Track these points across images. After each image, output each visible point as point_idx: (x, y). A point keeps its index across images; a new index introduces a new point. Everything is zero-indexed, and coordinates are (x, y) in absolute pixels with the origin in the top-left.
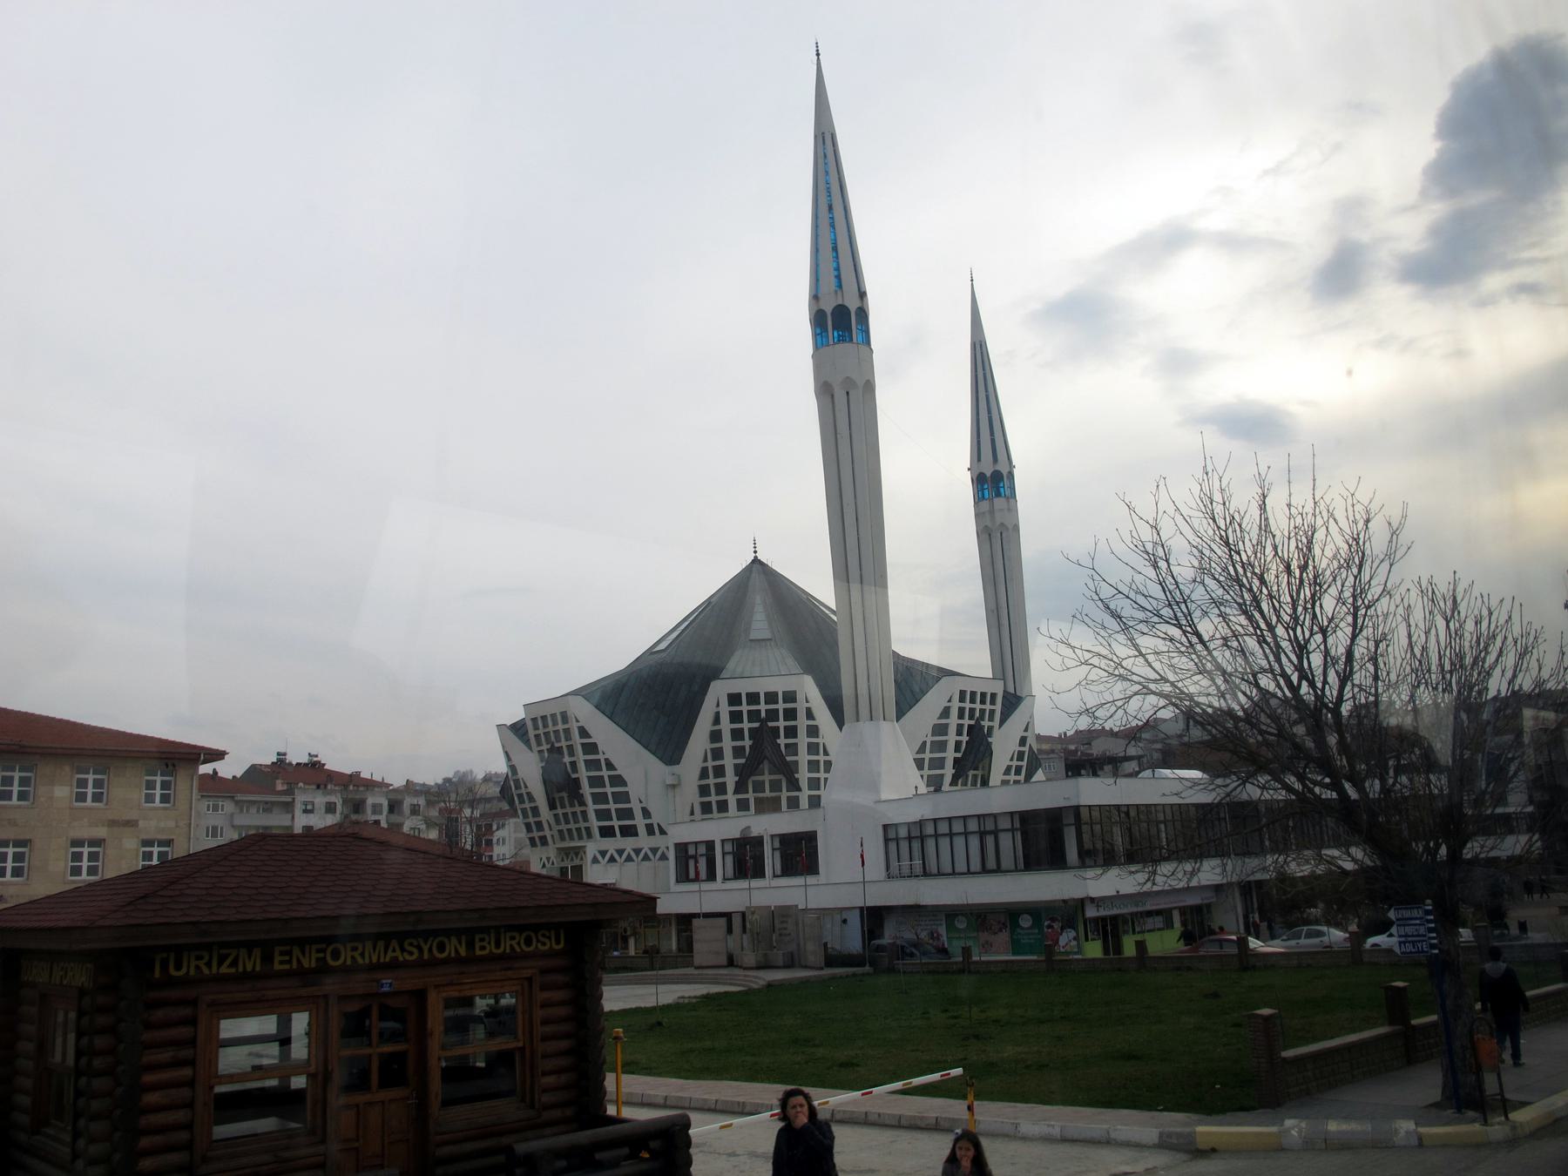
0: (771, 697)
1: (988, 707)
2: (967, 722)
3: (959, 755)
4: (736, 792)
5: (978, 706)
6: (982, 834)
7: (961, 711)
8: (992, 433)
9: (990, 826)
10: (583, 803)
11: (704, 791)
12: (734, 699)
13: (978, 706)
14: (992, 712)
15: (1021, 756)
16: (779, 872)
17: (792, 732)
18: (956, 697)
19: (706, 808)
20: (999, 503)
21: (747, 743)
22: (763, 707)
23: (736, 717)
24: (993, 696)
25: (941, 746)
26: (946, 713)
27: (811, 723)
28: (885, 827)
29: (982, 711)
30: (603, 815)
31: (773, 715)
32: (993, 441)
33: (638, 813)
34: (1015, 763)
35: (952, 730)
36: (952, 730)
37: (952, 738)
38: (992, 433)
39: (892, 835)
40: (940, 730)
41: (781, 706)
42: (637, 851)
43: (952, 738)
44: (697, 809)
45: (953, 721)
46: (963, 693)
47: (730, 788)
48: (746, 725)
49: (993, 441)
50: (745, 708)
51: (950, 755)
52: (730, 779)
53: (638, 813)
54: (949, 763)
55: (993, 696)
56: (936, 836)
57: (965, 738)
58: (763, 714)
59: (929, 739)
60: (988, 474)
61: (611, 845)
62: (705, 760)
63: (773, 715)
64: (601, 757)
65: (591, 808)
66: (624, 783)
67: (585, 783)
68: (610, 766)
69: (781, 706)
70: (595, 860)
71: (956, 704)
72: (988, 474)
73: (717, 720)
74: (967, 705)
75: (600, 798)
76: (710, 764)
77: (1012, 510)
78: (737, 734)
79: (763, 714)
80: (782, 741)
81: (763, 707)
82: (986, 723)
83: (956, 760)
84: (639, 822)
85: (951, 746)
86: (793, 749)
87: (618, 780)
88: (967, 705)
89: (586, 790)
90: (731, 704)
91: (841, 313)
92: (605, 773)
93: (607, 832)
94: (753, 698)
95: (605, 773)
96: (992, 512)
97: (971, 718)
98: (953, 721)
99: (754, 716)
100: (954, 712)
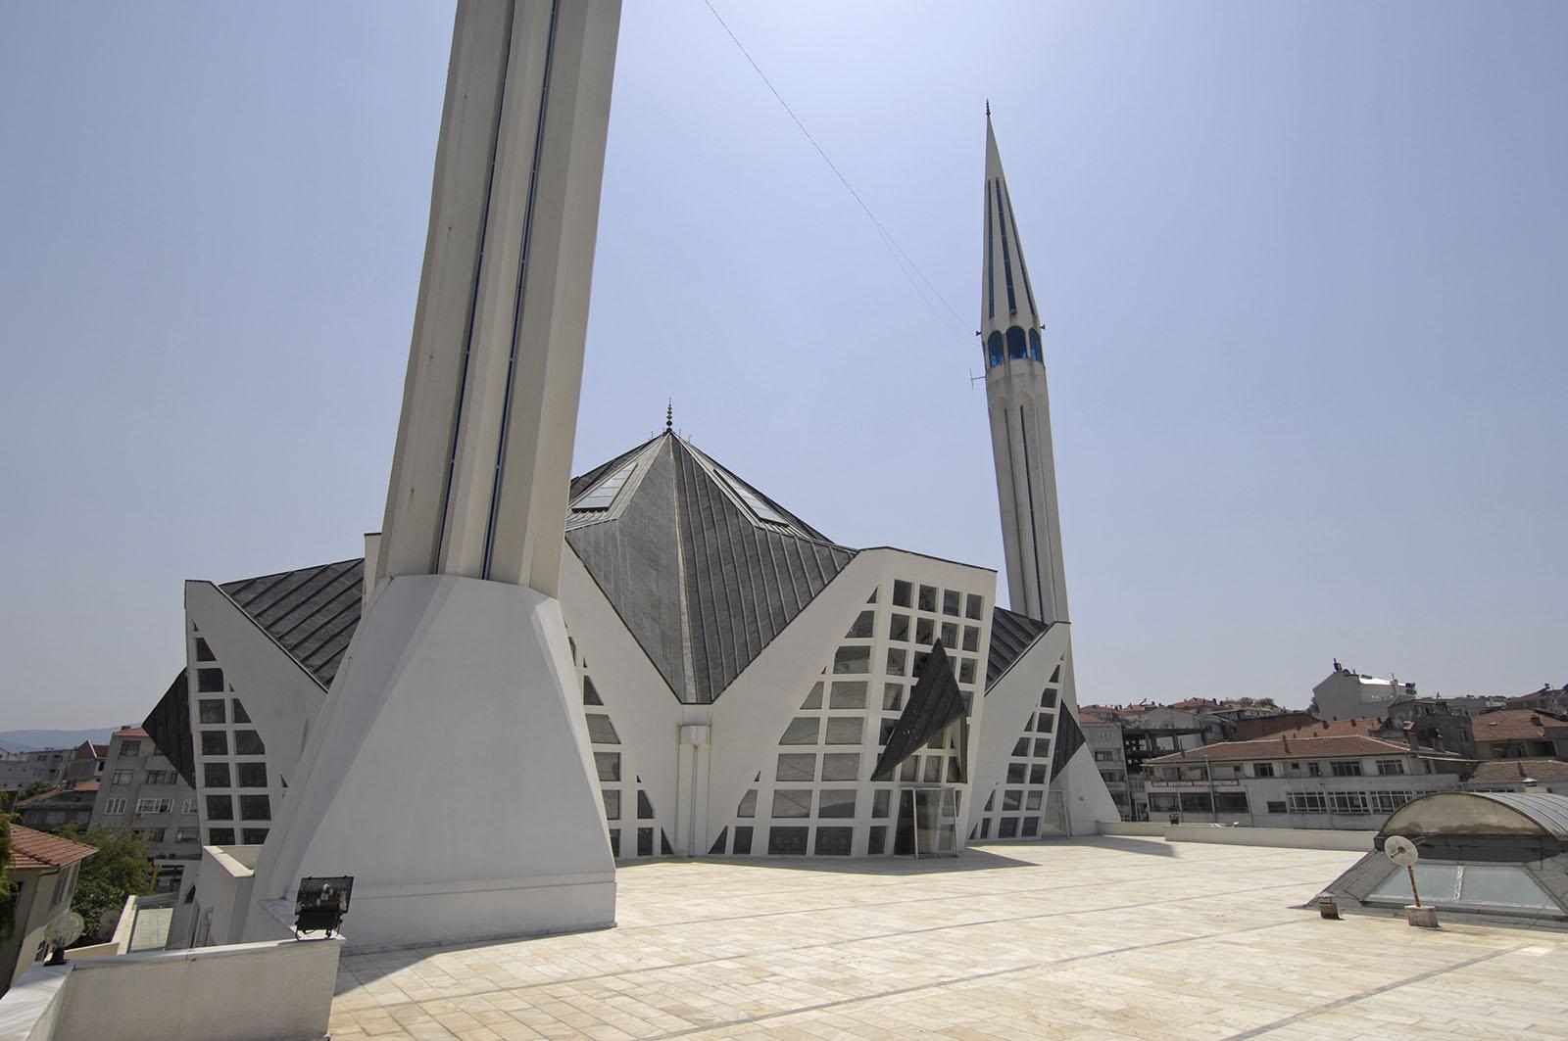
1: (962, 621)
2: (912, 647)
5: (939, 618)
7: (899, 630)
8: (1009, 282)
13: (939, 618)
14: (972, 636)
15: (1045, 724)
18: (887, 594)
20: (1018, 365)
25: (851, 694)
26: (864, 626)
29: (949, 630)
32: (1011, 292)
34: (1035, 735)
35: (879, 659)
36: (879, 659)
37: (877, 677)
38: (1009, 282)
43: (877, 677)
45: (881, 642)
49: (1011, 292)
51: (875, 716)
57: (909, 681)
59: (830, 678)
60: (1004, 332)
64: (226, 696)
66: (260, 749)
68: (241, 716)
71: (885, 611)
72: (1004, 332)
74: (914, 613)
75: (217, 775)
77: (1037, 378)
82: (957, 654)
83: (888, 730)
85: (876, 694)
87: (250, 742)
88: (914, 613)
89: (200, 759)
95: (230, 727)
96: (1008, 379)
98: (881, 642)
100: (882, 626)
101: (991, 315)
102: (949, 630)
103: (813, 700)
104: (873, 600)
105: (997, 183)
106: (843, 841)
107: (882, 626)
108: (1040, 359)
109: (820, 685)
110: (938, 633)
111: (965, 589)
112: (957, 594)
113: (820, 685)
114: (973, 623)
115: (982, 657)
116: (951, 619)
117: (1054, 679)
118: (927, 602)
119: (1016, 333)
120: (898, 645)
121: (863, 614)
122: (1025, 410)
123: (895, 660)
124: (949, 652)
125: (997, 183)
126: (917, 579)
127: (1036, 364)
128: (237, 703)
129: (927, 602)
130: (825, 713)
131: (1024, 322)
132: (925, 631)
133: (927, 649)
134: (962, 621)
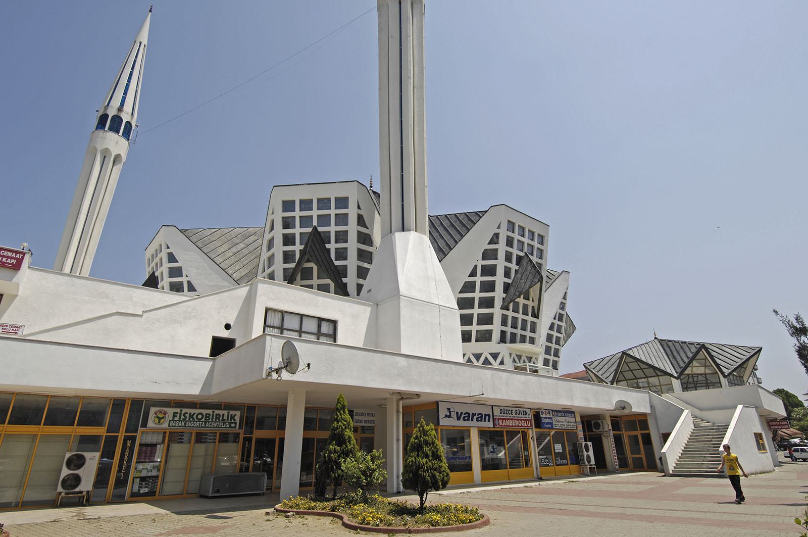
0: (324, 203)
5: (526, 240)
17: (342, 237)
18: (504, 226)
21: (298, 248)
22: (315, 213)
25: (489, 271)
26: (495, 239)
31: (323, 220)
35: (501, 255)
36: (501, 255)
43: (500, 263)
45: (502, 247)
54: (499, 288)
64: (184, 279)
69: (333, 212)
78: (288, 240)
80: (332, 246)
86: (342, 254)
88: (516, 236)
94: (306, 204)
98: (502, 247)
99: (305, 221)
100: (503, 240)
103: (473, 274)
104: (499, 227)
106: (487, 336)
107: (503, 240)
109: (476, 266)
111: (537, 230)
113: (476, 266)
123: (508, 258)
126: (518, 221)
128: (189, 282)
130: (479, 279)
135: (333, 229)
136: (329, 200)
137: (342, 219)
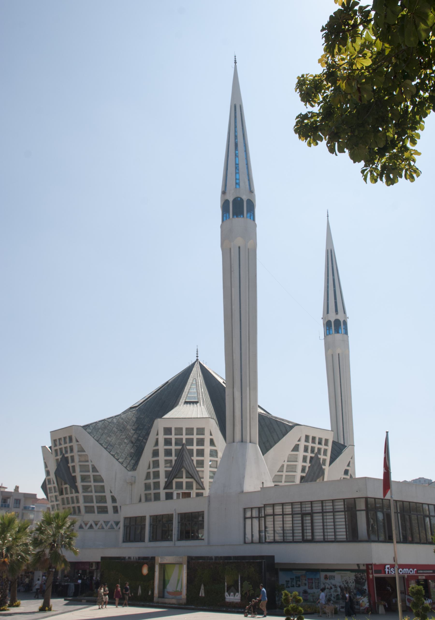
2: (309, 455)
3: (304, 475)
4: (165, 488)
5: (317, 446)
6: (303, 515)
7: (306, 450)
8: (335, 299)
9: (308, 509)
10: (77, 491)
11: (147, 487)
12: (168, 431)
13: (317, 446)
14: (325, 451)
16: (179, 538)
17: (201, 453)
18: (303, 439)
19: (147, 499)
21: (173, 458)
22: (184, 437)
23: (168, 442)
24: (327, 441)
26: (296, 448)
27: (213, 448)
28: (245, 510)
29: (319, 450)
30: (87, 499)
33: (109, 500)
37: (300, 464)
38: (335, 299)
39: (248, 514)
40: (292, 459)
41: (195, 437)
42: (106, 523)
44: (143, 499)
45: (301, 453)
46: (307, 437)
47: (162, 485)
48: (173, 447)
50: (173, 437)
51: (299, 474)
52: (162, 480)
53: (109, 500)
55: (327, 441)
56: (274, 515)
57: (308, 465)
58: (184, 441)
59: (286, 463)
61: (90, 518)
62: (149, 468)
63: (190, 442)
64: (90, 464)
65: (81, 496)
66: (102, 481)
67: (79, 479)
68: (94, 469)
69: (195, 437)
70: (81, 527)
71: (302, 444)
73: (157, 444)
74: (310, 445)
76: (152, 470)
78: (168, 453)
79: (184, 441)
80: (195, 458)
81: (184, 437)
82: (322, 457)
84: (109, 504)
85: (299, 469)
86: (201, 463)
88: (310, 445)
89: (79, 484)
90: (165, 434)
91: (238, 202)
92: (91, 474)
93: (90, 510)
95: (91, 474)
97: (312, 451)
100: (302, 448)
101: (328, 313)
102: (319, 450)
103: (281, 470)
104: (299, 441)
105: (331, 251)
107: (302, 448)
108: (346, 333)
109: (283, 466)
110: (316, 450)
112: (322, 438)
113: (283, 466)
114: (326, 447)
115: (328, 458)
116: (320, 446)
117: (348, 465)
118: (314, 442)
119: (337, 322)
120: (306, 454)
121: (296, 445)
122: (340, 355)
124: (319, 456)
125: (331, 251)
127: (345, 336)
129: (314, 442)
131: (340, 317)
132: (313, 451)
133: (313, 455)
134: (323, 447)
135: (195, 447)
136: (192, 429)
137: (201, 442)
